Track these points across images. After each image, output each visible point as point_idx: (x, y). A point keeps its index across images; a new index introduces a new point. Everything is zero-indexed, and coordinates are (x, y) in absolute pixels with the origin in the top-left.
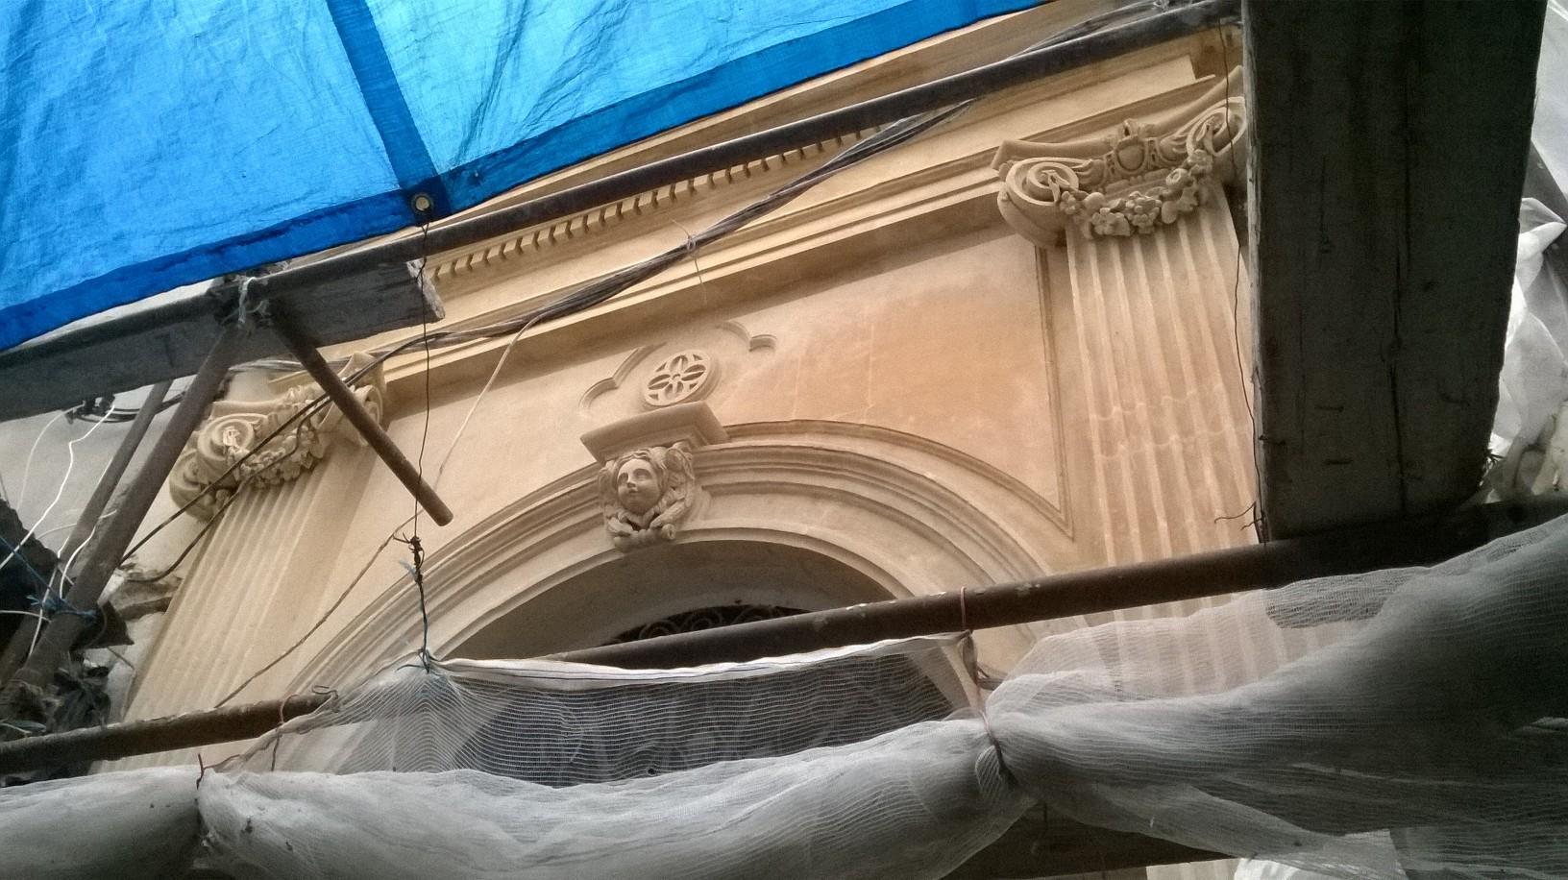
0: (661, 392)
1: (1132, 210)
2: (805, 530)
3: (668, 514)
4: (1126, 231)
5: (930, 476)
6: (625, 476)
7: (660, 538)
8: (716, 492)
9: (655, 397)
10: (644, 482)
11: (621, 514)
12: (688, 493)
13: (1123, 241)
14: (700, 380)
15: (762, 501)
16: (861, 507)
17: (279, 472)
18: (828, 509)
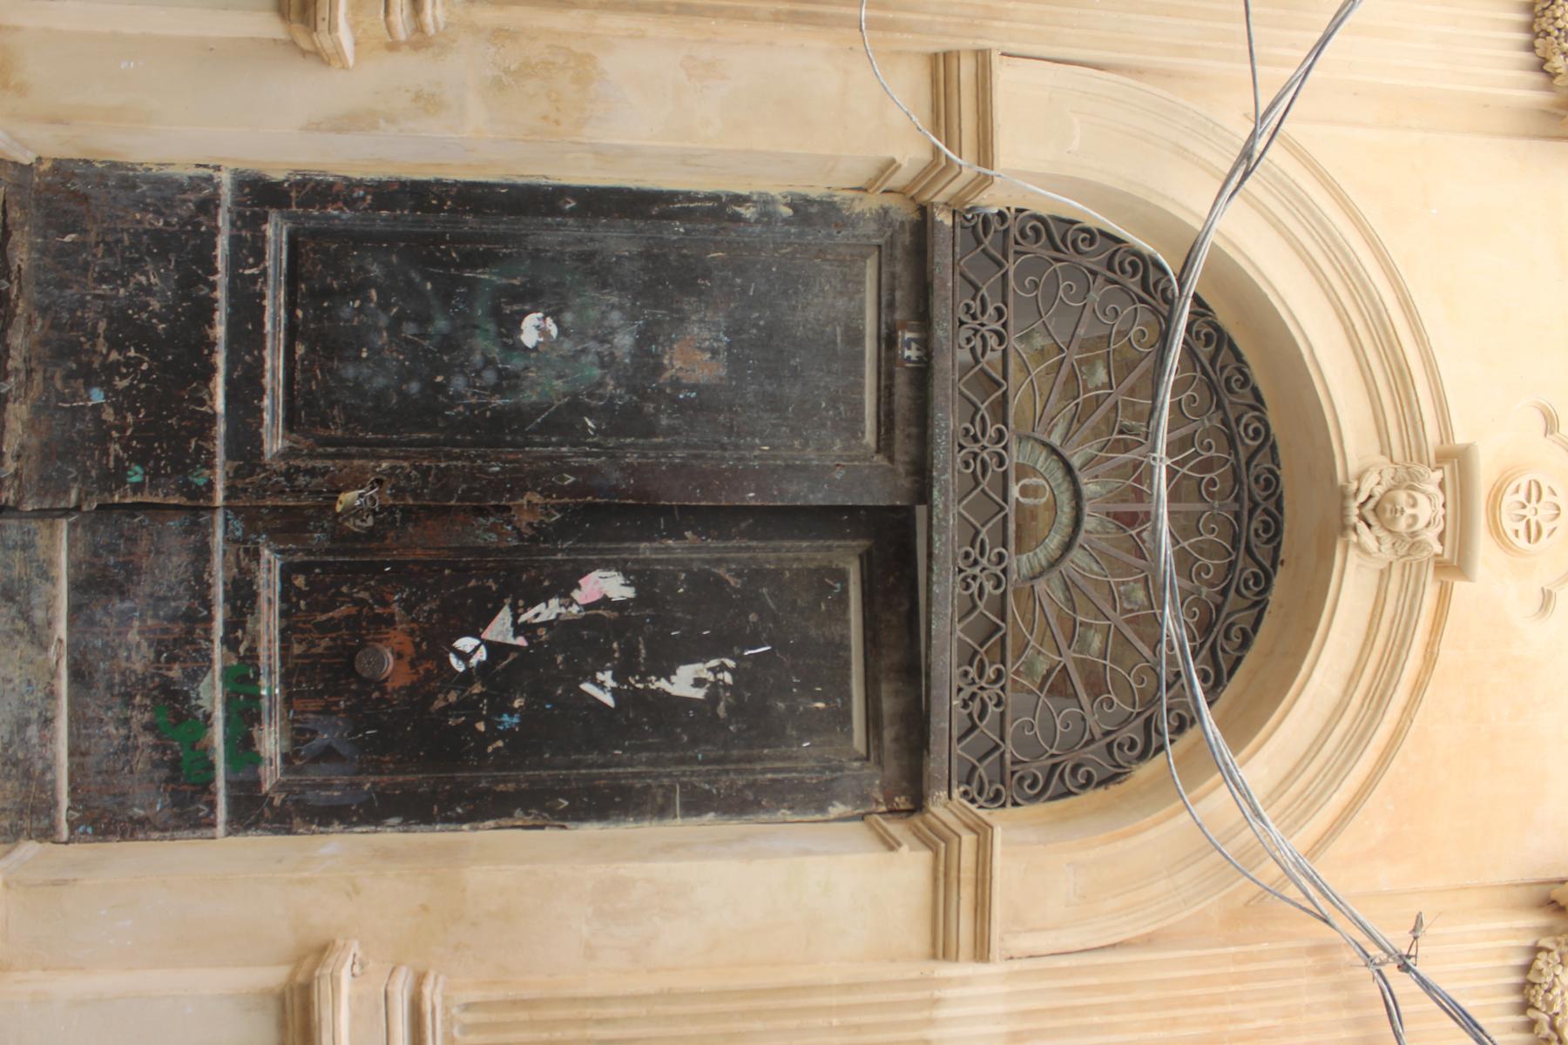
0: (1522, 497)
1: (1548, 991)
2: (1316, 675)
3: (1367, 537)
4: (1532, 977)
5: (1336, 796)
6: (1414, 505)
7: (1344, 528)
8: (1384, 575)
9: (1517, 491)
10: (1402, 525)
11: (1378, 491)
12: (1387, 552)
13: (1527, 968)
14: (1521, 542)
15: (1362, 623)
16: (1327, 723)
17: (1549, 34)
18: (1335, 691)
